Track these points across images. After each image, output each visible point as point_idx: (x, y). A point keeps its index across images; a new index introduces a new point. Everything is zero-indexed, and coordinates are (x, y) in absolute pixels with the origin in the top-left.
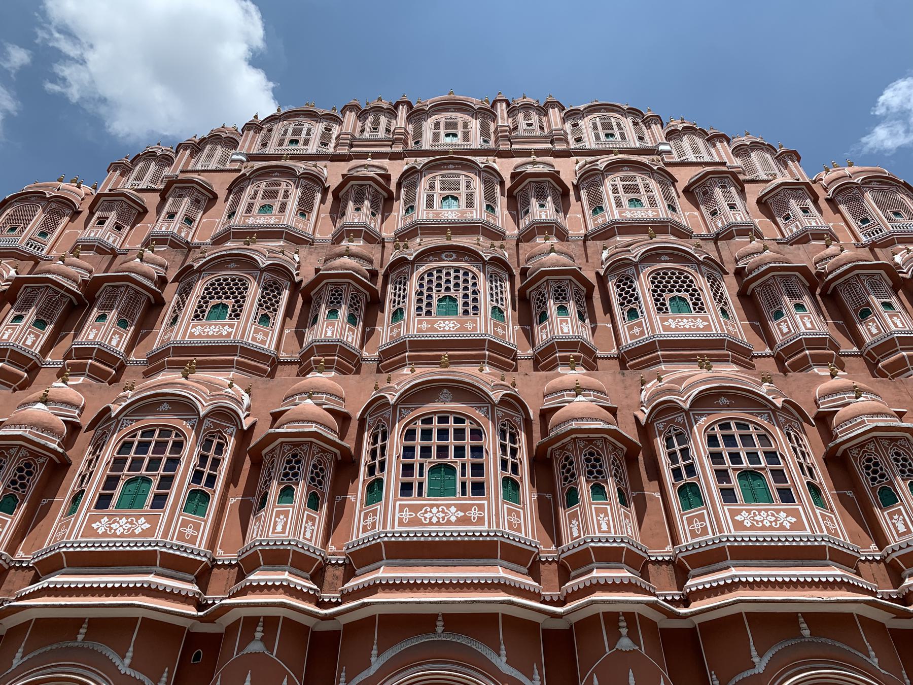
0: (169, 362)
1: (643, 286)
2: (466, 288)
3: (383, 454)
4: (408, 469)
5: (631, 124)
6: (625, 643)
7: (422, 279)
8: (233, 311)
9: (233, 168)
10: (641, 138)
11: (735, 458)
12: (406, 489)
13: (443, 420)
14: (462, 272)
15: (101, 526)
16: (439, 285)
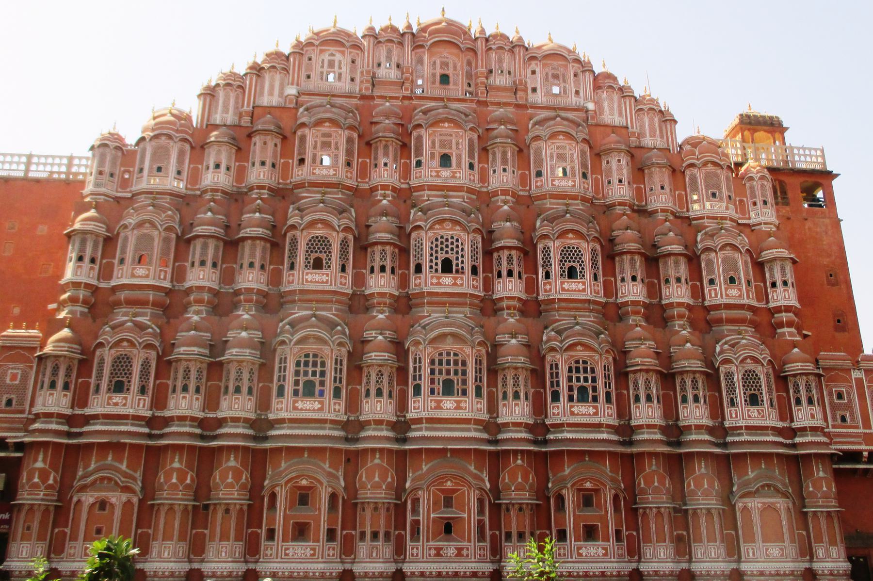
0: (299, 300)
1: (555, 257)
2: (457, 253)
3: (420, 371)
4: (432, 382)
5: (572, 77)
6: (519, 462)
7: (432, 243)
8: (327, 263)
9: (291, 106)
10: (577, 93)
11: (578, 379)
12: (432, 392)
13: (448, 354)
14: (455, 238)
15: (300, 405)
16: (442, 249)
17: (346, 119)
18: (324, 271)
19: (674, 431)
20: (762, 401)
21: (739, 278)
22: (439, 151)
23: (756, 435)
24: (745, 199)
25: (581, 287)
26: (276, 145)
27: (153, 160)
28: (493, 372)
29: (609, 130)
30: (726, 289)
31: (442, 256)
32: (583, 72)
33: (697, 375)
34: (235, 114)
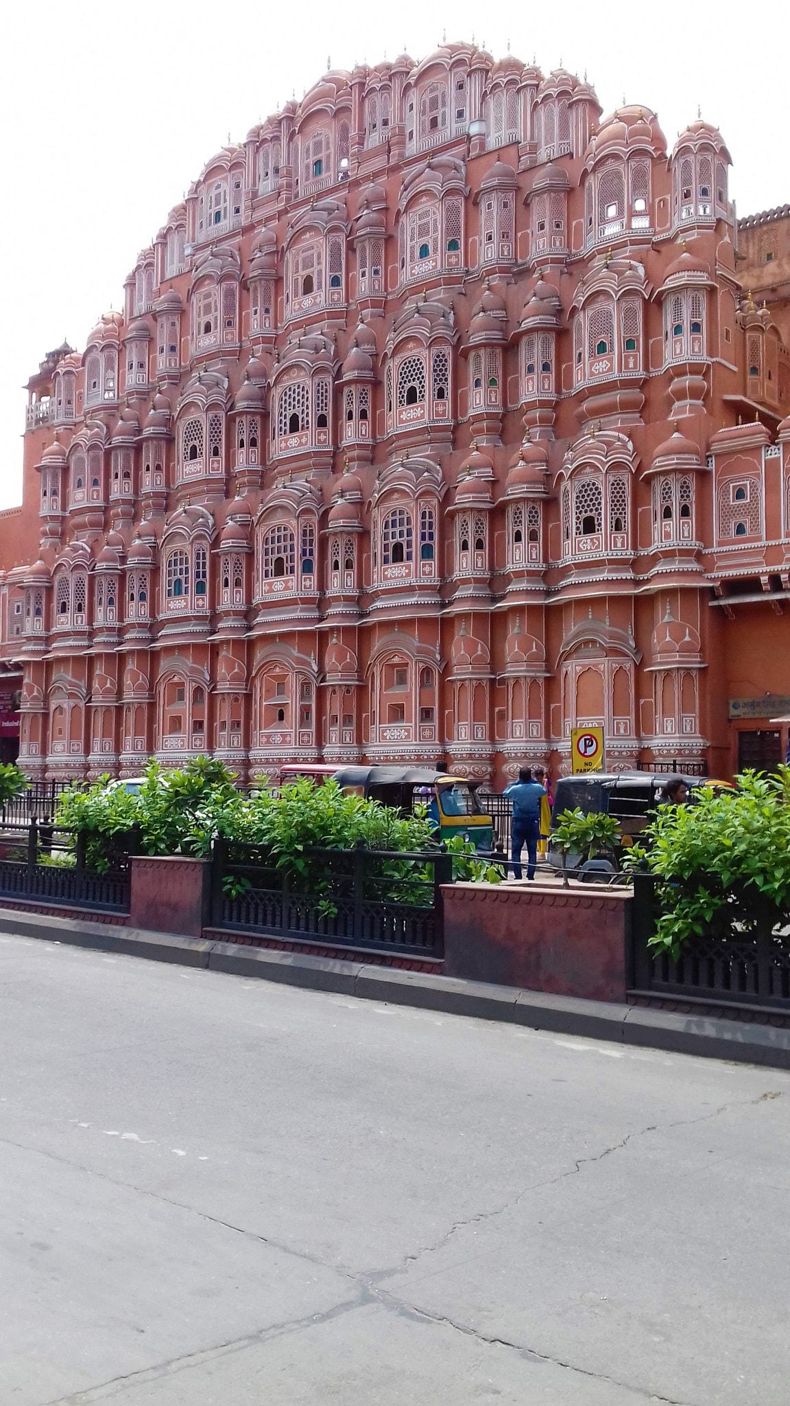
1: (395, 378)
10: (460, 114)
15: (172, 605)
17: (222, 269)
18: (197, 460)
19: (495, 583)
20: (600, 525)
21: (611, 343)
22: (304, 273)
23: (593, 573)
24: (668, 197)
25: (419, 412)
26: (173, 324)
27: (90, 378)
28: (323, 541)
29: (495, 156)
30: (591, 365)
31: (289, 414)
32: (469, 75)
33: (521, 505)
34: (149, 299)
